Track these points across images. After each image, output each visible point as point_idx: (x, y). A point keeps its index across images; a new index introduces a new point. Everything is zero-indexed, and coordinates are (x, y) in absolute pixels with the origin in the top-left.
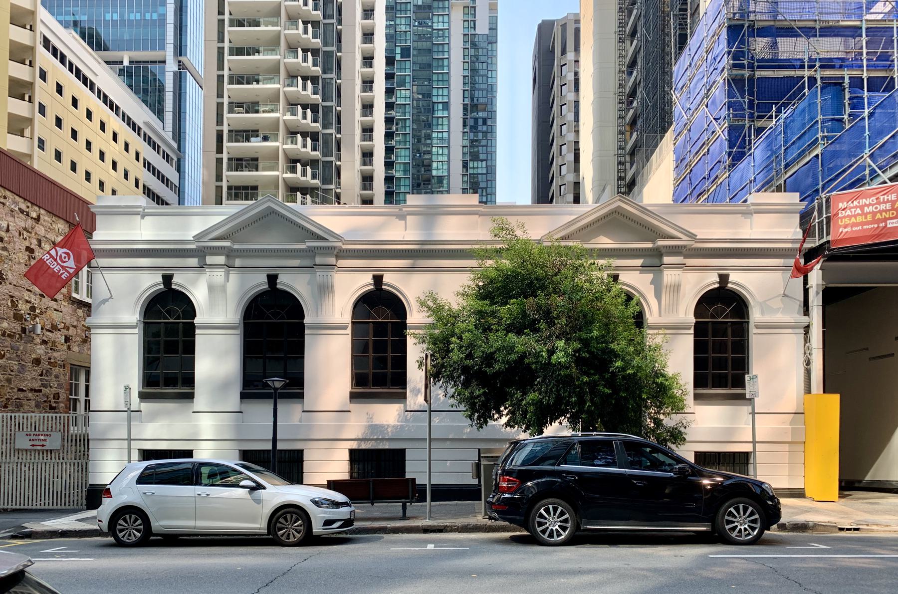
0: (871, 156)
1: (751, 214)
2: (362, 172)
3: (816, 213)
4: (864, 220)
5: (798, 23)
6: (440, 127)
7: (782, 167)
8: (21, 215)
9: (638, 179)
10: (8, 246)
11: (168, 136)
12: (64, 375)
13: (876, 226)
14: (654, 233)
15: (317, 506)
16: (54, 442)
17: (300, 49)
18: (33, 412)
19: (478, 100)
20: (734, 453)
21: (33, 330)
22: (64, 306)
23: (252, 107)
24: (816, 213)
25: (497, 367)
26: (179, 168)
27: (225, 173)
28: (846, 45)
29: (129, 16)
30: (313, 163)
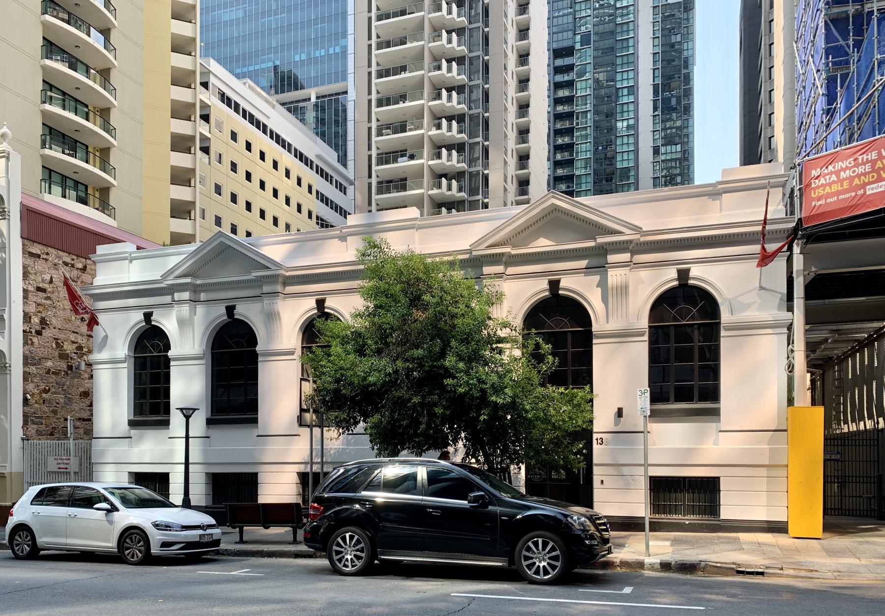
1: (721, 194)
4: (840, 189)
6: (625, 114)
8: (65, 267)
13: (853, 194)
15: (157, 529)
20: (684, 478)
21: (78, 368)
29: (314, 53)
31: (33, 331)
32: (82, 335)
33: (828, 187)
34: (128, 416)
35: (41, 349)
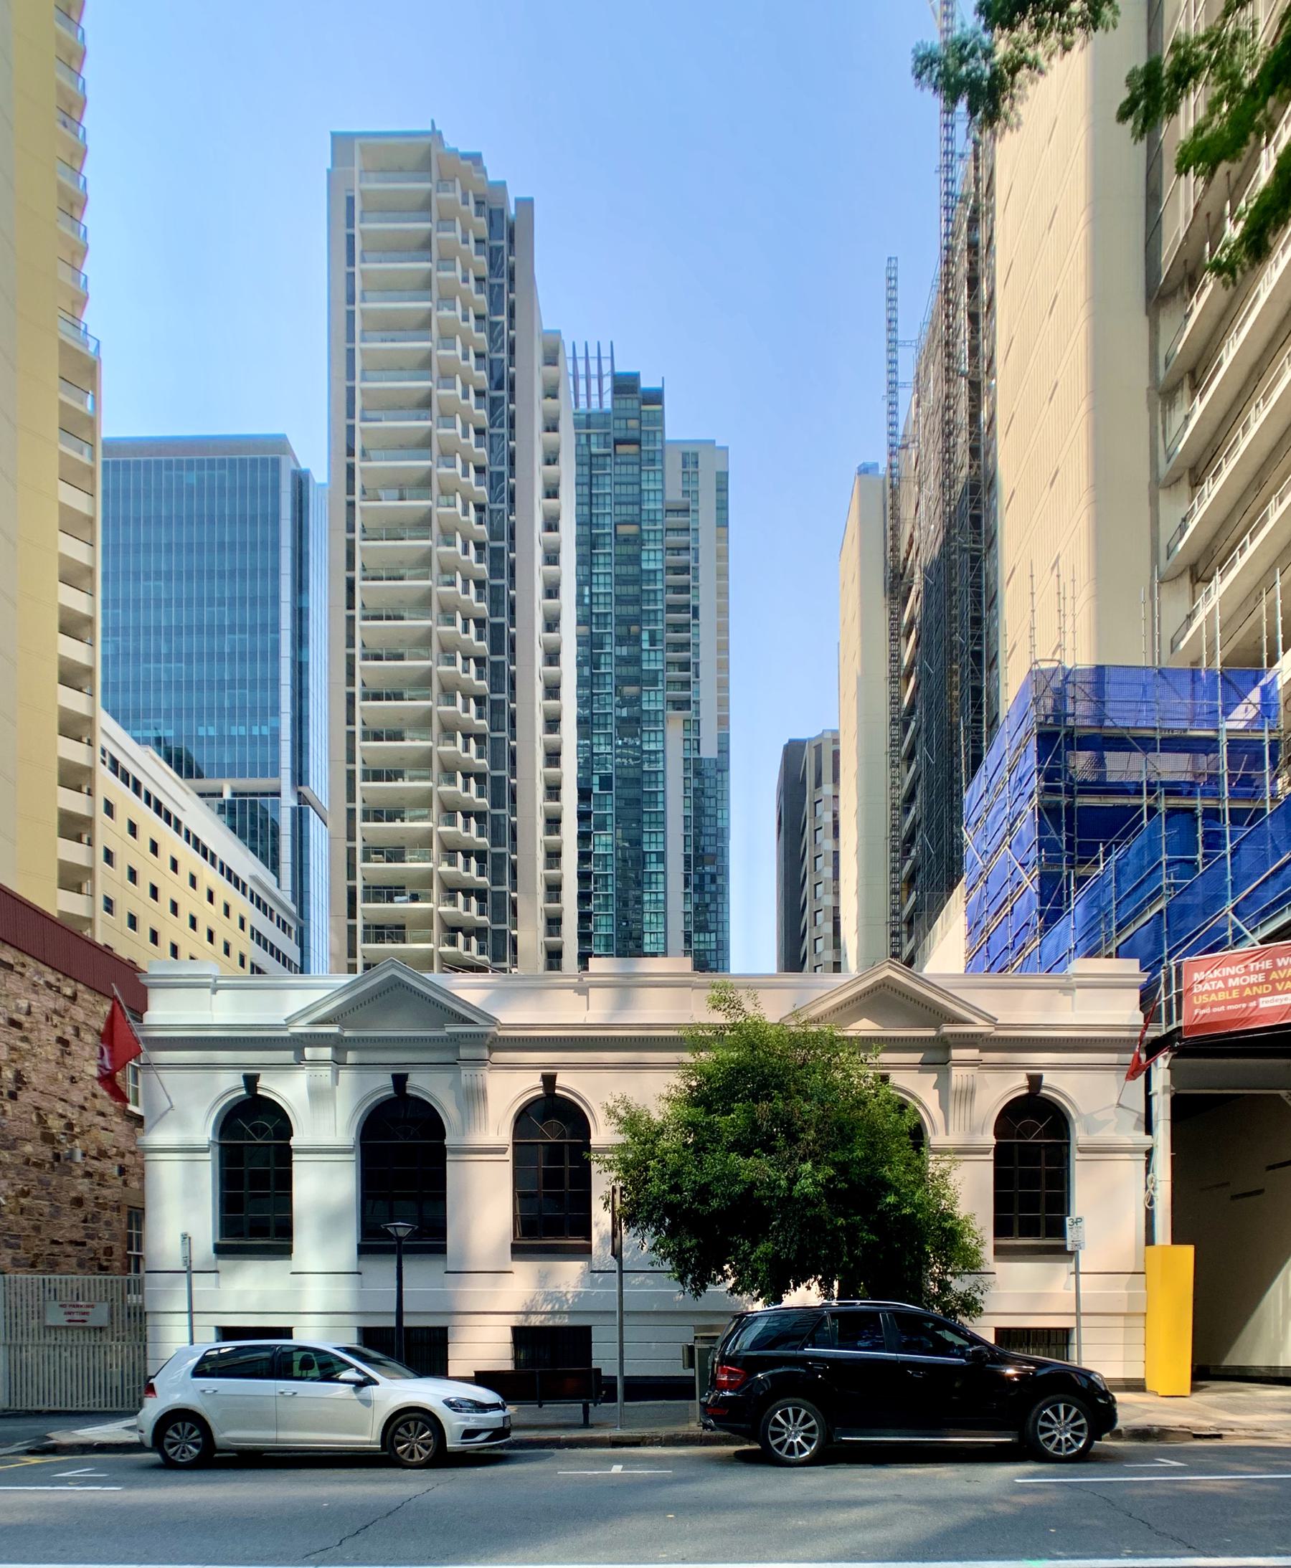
0: (1235, 910)
1: (1072, 989)
2: (547, 945)
3: (1162, 988)
5: (1132, 732)
7: (1113, 928)
9: (919, 953)
10: (30, 1036)
11: (286, 896)
12: (120, 1221)
13: (1244, 1005)
14: (937, 1015)
16: (100, 1315)
17: (459, 774)
18: (73, 1273)
19: (703, 850)
20: (1049, 1330)
21: (71, 1157)
22: (116, 1123)
23: (396, 855)
24: (1162, 988)
25: (715, 1203)
26: (302, 942)
27: (360, 946)
28: (1195, 763)
30: (480, 932)
31: (5, 1091)
32: (73, 1106)
33: (1213, 995)
34: (214, 1237)
35: (17, 1123)
